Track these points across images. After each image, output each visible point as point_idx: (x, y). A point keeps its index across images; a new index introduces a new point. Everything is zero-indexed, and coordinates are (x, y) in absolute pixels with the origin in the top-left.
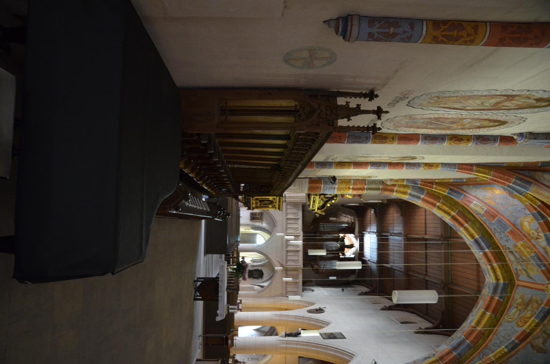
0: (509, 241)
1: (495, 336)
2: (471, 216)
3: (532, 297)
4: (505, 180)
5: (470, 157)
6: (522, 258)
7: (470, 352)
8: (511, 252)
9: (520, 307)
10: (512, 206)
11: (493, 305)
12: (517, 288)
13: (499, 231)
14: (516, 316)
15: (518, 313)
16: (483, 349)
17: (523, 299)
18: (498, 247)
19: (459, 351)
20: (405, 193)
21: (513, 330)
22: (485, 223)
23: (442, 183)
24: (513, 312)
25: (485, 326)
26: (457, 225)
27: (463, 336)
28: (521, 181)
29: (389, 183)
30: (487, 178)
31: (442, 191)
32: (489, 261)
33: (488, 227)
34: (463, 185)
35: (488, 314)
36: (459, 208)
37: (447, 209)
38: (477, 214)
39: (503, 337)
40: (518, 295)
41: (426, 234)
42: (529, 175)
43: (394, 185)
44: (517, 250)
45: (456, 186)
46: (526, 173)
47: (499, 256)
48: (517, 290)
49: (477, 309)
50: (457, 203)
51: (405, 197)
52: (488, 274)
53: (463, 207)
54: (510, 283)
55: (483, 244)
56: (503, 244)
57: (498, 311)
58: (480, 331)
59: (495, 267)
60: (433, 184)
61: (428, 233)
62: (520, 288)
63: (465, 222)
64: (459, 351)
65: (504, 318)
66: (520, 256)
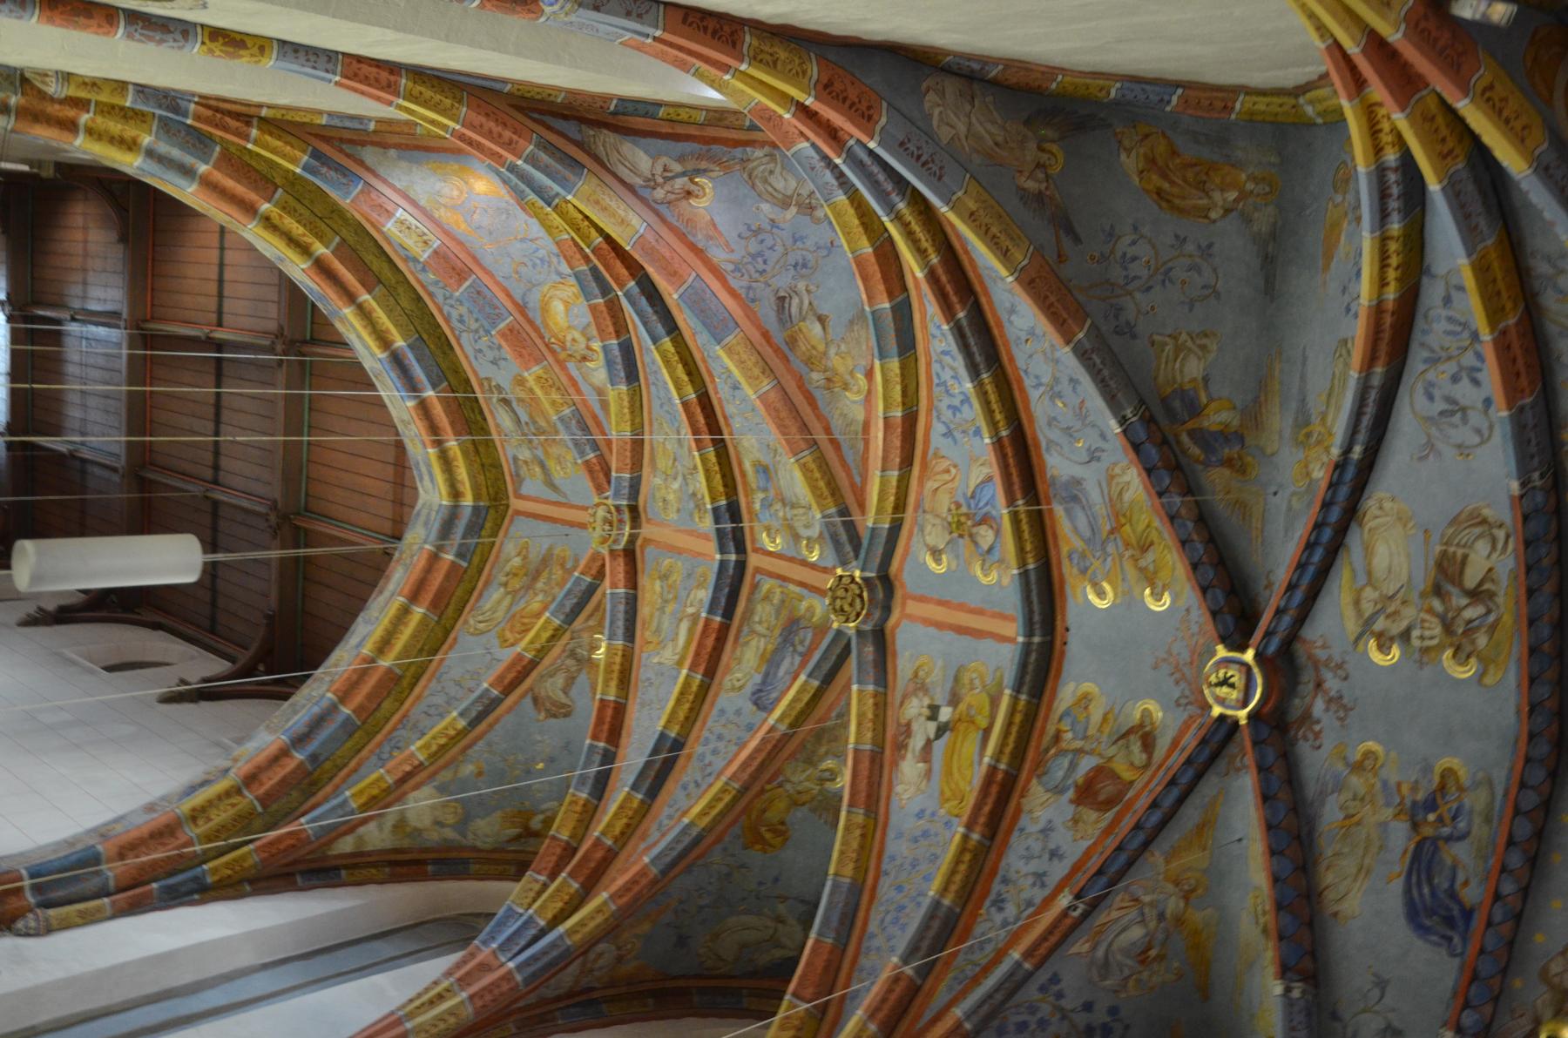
0: (502, 363)
1: (433, 684)
2: (385, 266)
3: (551, 548)
4: (502, 145)
5: (390, 35)
6: (535, 422)
7: (349, 744)
10: (523, 240)
11: (437, 580)
12: (511, 521)
13: (474, 326)
14: (500, 614)
15: (508, 599)
16: (394, 729)
17: (525, 558)
18: (467, 381)
19: (312, 747)
20: (131, 145)
21: (489, 657)
22: (431, 295)
23: (284, 126)
24: (493, 600)
25: (405, 653)
26: (331, 293)
27: (329, 695)
28: (552, 155)
29: (52, 88)
30: (445, 127)
31: (284, 156)
32: (434, 429)
33: (440, 310)
34: (363, 144)
35: (419, 611)
36: (344, 232)
37: (298, 230)
38: (406, 259)
39: (458, 684)
40: (517, 544)
41: (220, 324)
42: (578, 137)
43: (81, 104)
44: (522, 395)
45: (336, 144)
46: (571, 128)
47: (468, 415)
48: (512, 529)
49: (381, 599)
50: (336, 211)
51: (131, 164)
52: (426, 478)
53: (359, 229)
54: (494, 507)
55: (418, 372)
56: (482, 375)
57: (449, 599)
58: (389, 671)
59: (451, 453)
60: (248, 124)
61: (227, 319)
62: (521, 522)
63: (363, 285)
64: (312, 747)
65: (466, 622)
66: (531, 417)
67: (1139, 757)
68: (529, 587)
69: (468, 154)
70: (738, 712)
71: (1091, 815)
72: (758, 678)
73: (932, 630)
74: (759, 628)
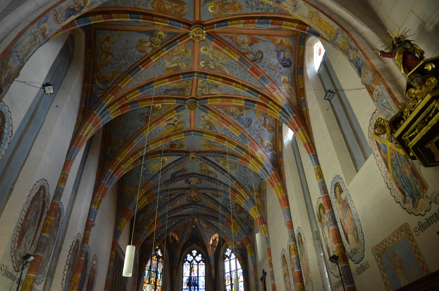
3: (185, 3)
69: (309, 35)
70: (162, 89)
71: (169, 147)
72: (170, 88)
73: (189, 115)
74: (181, 84)
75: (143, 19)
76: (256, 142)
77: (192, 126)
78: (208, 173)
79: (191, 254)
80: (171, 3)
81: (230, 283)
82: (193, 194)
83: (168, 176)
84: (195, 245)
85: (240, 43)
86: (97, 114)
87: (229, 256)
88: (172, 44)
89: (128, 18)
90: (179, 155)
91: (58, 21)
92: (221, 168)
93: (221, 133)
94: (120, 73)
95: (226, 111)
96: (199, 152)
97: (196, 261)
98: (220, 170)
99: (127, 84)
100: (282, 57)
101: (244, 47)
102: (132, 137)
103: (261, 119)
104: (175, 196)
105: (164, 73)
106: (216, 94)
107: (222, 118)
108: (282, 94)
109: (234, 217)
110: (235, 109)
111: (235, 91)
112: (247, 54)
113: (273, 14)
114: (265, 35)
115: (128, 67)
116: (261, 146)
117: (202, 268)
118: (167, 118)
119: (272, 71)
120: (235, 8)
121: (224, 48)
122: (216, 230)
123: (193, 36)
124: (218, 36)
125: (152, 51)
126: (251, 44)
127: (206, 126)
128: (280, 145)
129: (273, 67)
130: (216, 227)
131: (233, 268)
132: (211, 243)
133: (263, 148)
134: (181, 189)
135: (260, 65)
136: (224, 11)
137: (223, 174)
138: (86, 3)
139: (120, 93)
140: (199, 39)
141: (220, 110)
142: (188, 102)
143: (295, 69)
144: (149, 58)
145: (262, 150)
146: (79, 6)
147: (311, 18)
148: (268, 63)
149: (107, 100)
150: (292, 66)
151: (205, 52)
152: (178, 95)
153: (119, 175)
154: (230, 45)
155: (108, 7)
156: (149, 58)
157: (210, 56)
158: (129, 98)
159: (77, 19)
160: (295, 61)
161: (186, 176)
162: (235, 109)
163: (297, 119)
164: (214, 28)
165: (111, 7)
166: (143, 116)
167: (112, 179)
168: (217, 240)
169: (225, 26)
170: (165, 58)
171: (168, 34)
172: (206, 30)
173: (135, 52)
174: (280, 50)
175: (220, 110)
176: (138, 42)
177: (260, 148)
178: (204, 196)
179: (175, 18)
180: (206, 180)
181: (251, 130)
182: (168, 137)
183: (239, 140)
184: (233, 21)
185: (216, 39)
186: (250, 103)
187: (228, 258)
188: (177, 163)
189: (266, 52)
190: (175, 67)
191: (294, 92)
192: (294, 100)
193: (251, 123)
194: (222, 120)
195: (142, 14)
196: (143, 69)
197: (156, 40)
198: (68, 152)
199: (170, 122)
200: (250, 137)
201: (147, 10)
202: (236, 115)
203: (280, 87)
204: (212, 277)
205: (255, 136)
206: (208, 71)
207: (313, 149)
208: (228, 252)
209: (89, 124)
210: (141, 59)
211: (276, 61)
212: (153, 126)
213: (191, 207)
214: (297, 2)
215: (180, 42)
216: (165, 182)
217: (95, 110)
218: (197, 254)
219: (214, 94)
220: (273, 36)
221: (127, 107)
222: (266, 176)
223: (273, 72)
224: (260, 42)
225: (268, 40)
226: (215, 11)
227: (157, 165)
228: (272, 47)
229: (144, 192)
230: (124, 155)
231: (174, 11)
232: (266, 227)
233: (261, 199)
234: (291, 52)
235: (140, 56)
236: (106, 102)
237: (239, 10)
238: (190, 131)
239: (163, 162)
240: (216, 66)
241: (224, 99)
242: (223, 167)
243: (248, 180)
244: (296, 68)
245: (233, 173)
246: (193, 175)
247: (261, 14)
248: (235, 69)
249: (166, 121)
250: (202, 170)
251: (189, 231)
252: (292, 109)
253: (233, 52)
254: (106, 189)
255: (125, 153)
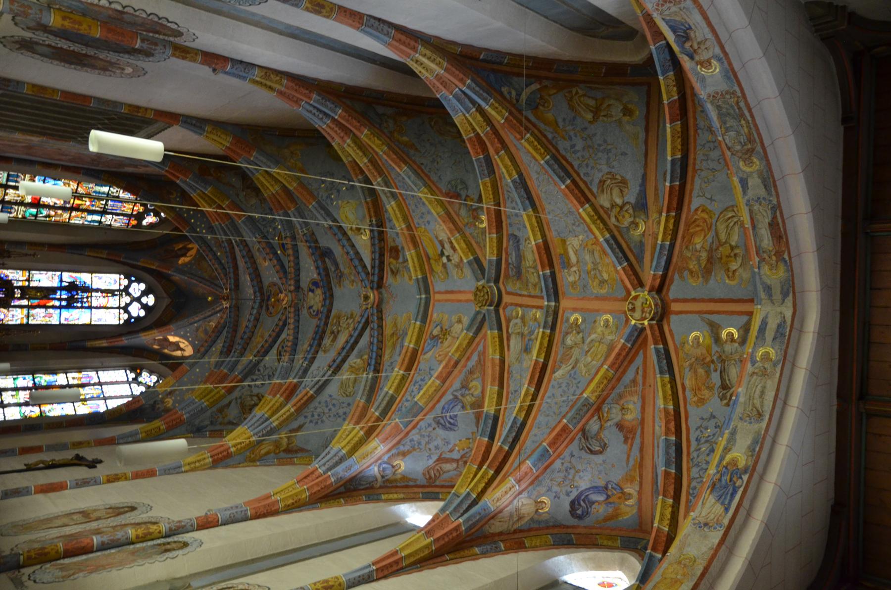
3: (707, 281)
6: (708, 373)
8: (725, 387)
9: (724, 250)
14: (721, 227)
15: (723, 237)
17: (728, 270)
67: (392, 266)
68: (711, 251)
70: (519, 229)
71: (392, 244)
72: (521, 247)
74: (532, 270)
75: (671, 187)
76: (401, 439)
77: (438, 297)
78: (333, 332)
79: (145, 293)
80: (708, 248)
81: (71, 382)
82: (285, 298)
83: (327, 241)
84: (167, 301)
85: (622, 402)
86: (464, 84)
87: (140, 379)
88: (617, 250)
89: (673, 154)
90: (373, 267)
91: (662, 5)
92: (344, 361)
93: (422, 361)
94: (554, 138)
95: (471, 372)
96: (380, 311)
97: (127, 305)
98: (340, 358)
99: (529, 152)
100: (594, 497)
101: (614, 411)
102: (414, 162)
103: (455, 452)
104: (282, 257)
105: (554, 233)
106: (509, 350)
107: (456, 363)
108: (510, 498)
109: (230, 390)
110: (476, 393)
111: (516, 391)
112: (599, 418)
113: (689, 475)
114: (642, 458)
115: (568, 156)
116: (394, 451)
117: (111, 318)
118: (456, 240)
119: (562, 475)
120: (699, 389)
121: (611, 366)
122: (203, 349)
123: (636, 298)
124: (637, 353)
125: (602, 207)
126: (620, 426)
127: (439, 327)
128: (395, 496)
129: (570, 477)
130: (207, 351)
131: (109, 390)
132: (172, 339)
133: (389, 458)
134: (298, 271)
135: (574, 447)
136: (691, 365)
137: (330, 367)
138: (702, 66)
139: (510, 137)
140: (629, 310)
141: (475, 357)
142: (490, 287)
143: (568, 527)
144: (588, 200)
145: (384, 454)
146: (695, 51)
147: (679, 563)
148: (579, 467)
149: (495, 109)
150: (574, 522)
151: (602, 323)
152: (508, 264)
153: (329, 130)
154: (619, 380)
155: (695, 112)
156: (588, 200)
157: (593, 336)
158: (499, 157)
159: (668, 45)
160: (585, 527)
161: (326, 283)
162: (476, 393)
163: (455, 534)
164: (656, 343)
165: (695, 119)
166: (460, 187)
167: (321, 116)
168: (178, 353)
169: (660, 367)
170: (587, 236)
171: (641, 241)
172: (651, 326)
173: (600, 170)
174: (610, 493)
175: (475, 357)
176: (622, 177)
177: (389, 450)
178: (281, 323)
179: (674, 259)
180: (318, 326)
181: (430, 429)
182: (415, 243)
183: (407, 400)
184: (672, 387)
185: (630, 349)
186: (490, 425)
187: (135, 380)
188: (356, 262)
189: (604, 461)
190: (569, 259)
191: (515, 527)
192: (496, 527)
193: (445, 427)
194: (452, 363)
195: (683, 186)
196: (563, 187)
197: (627, 215)
198: (379, 20)
199: (447, 246)
200: (414, 428)
201: (691, 197)
202: (463, 396)
203: (525, 494)
204: (90, 340)
205: (416, 438)
206: (560, 332)
207: (386, 573)
208: (148, 379)
209: (441, 67)
210: (585, 183)
211: (584, 483)
212: (439, 209)
213: (255, 293)
214: (715, 528)
215: (623, 269)
216: (313, 234)
217: (472, 80)
218: (144, 306)
219: (508, 346)
220: (641, 476)
221: (479, 150)
222: (324, 465)
223: (559, 477)
224: (626, 447)
225: (631, 465)
226: (692, 346)
227: (351, 217)
228: (616, 476)
229: (291, 188)
230: (373, 143)
231: (689, 255)
232: (204, 465)
233: (272, 455)
234: (607, 519)
235: (592, 181)
236: (491, 106)
237: (695, 399)
238: (427, 291)
239: (359, 229)
240: (571, 348)
241: (498, 368)
242: (346, 366)
243: (317, 423)
244: (570, 531)
245: (332, 389)
246: (329, 297)
247: (688, 447)
248: (564, 392)
249: (449, 238)
250: (338, 317)
251: (201, 288)
252: (478, 521)
253: (602, 386)
254: (297, 102)
255: (378, 146)
